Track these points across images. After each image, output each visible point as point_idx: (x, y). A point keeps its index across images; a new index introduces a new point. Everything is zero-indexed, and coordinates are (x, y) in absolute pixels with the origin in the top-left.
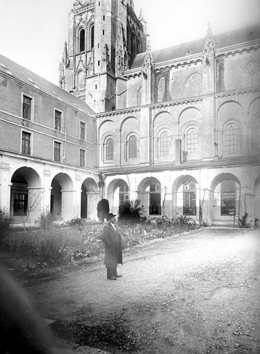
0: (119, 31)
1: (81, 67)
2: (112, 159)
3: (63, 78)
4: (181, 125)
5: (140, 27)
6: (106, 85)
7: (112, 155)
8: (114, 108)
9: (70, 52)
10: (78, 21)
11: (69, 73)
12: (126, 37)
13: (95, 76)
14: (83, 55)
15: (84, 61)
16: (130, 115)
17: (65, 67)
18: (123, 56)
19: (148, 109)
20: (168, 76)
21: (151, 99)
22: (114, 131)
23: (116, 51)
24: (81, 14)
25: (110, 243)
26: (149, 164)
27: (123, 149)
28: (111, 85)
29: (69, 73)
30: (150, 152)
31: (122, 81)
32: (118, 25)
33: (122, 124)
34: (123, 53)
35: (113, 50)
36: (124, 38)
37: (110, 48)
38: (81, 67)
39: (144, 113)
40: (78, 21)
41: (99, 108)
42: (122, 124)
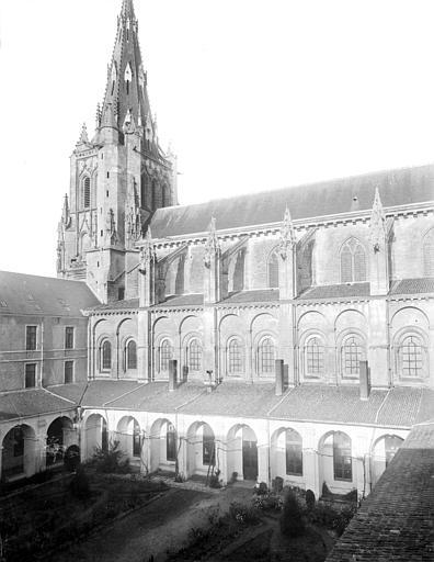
0: (130, 188)
1: (85, 228)
2: (109, 367)
3: (62, 244)
4: (183, 334)
5: (167, 167)
6: (109, 264)
7: (110, 362)
8: (121, 296)
9: (72, 207)
10: (81, 168)
11: (70, 236)
12: (139, 194)
13: (96, 249)
14: (88, 214)
15: (89, 223)
16: (127, 316)
17: (64, 228)
18: (134, 221)
19: (146, 312)
20: (185, 254)
21: (151, 299)
22: (110, 333)
23: (127, 213)
24: (84, 159)
25: (119, 517)
26: (147, 382)
27: (121, 357)
28: (117, 261)
29: (70, 236)
30: (149, 365)
31: (133, 255)
32: (129, 179)
33: (119, 326)
34: (135, 217)
35: (122, 216)
36: (136, 197)
37: (116, 213)
38: (85, 228)
39: (142, 316)
40: (81, 168)
41: (101, 295)
42: (119, 326)
